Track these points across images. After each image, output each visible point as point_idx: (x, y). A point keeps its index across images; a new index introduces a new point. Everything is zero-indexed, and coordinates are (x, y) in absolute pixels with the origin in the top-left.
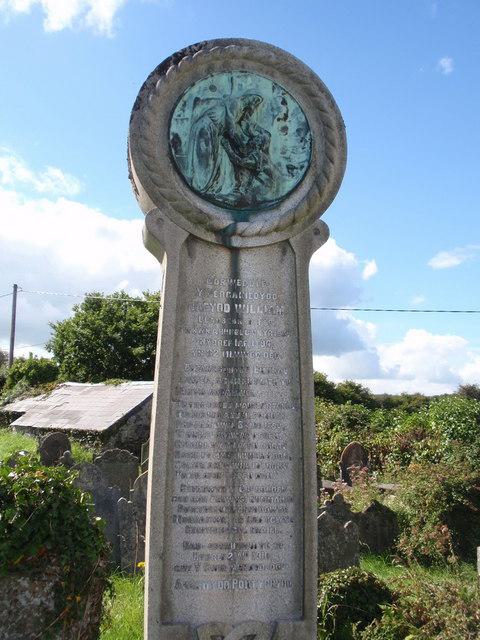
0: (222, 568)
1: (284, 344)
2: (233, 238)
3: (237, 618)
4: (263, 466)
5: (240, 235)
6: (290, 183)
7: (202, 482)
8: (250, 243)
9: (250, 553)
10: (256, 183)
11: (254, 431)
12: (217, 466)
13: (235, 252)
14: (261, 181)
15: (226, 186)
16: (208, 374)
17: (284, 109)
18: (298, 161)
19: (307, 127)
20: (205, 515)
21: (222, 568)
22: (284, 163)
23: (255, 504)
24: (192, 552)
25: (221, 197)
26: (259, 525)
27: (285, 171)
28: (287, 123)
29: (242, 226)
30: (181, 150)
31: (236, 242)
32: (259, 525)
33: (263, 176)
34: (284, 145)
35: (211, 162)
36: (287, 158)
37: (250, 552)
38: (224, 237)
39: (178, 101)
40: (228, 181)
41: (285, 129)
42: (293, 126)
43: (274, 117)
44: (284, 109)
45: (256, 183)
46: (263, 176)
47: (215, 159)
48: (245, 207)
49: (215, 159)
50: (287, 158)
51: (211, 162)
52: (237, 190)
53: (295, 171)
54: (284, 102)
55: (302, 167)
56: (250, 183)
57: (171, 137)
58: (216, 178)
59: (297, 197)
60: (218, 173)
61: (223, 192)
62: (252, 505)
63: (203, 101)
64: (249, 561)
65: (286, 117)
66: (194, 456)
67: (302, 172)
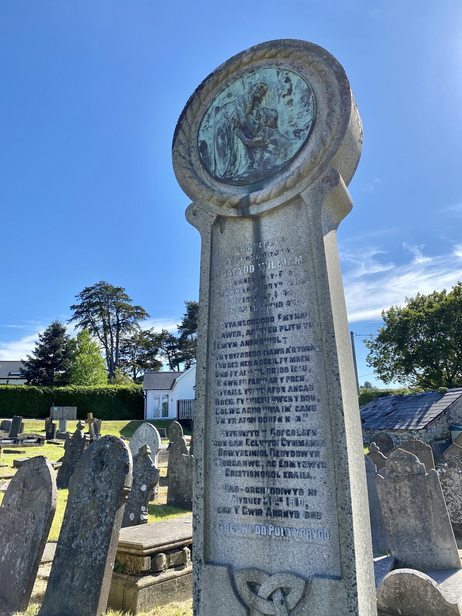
0: (259, 512)
1: (305, 290)
2: (251, 208)
3: (275, 566)
4: (292, 409)
5: (255, 203)
6: (298, 144)
7: (239, 427)
8: (266, 207)
9: (284, 499)
10: (267, 155)
11: (281, 375)
12: (249, 410)
13: (256, 219)
14: (270, 152)
15: (242, 167)
16: (239, 328)
17: (287, 86)
18: (303, 124)
19: (310, 90)
20: (237, 459)
21: (259, 512)
22: (292, 129)
23: (287, 448)
24: (231, 494)
25: (237, 177)
26: (292, 470)
27: (292, 136)
28: (292, 96)
29: (253, 196)
30: (207, 152)
31: (253, 211)
32: (292, 470)
33: (271, 147)
34: (291, 113)
35: (228, 152)
36: (293, 125)
37: (284, 497)
38: (243, 208)
39: (205, 113)
40: (244, 162)
41: (290, 102)
42: (296, 97)
43: (279, 96)
44: (287, 86)
45: (267, 155)
46: (271, 147)
47: (231, 149)
48: (256, 180)
49: (231, 149)
50: (293, 125)
51: (228, 152)
52: (251, 166)
53: (302, 133)
54: (288, 80)
55: (307, 127)
56: (262, 157)
57: (199, 144)
58: (233, 163)
59: (305, 154)
60: (236, 160)
61: (240, 173)
62: (283, 449)
63: (222, 107)
64: (283, 507)
65: (290, 91)
66: (231, 402)
67: (307, 132)
